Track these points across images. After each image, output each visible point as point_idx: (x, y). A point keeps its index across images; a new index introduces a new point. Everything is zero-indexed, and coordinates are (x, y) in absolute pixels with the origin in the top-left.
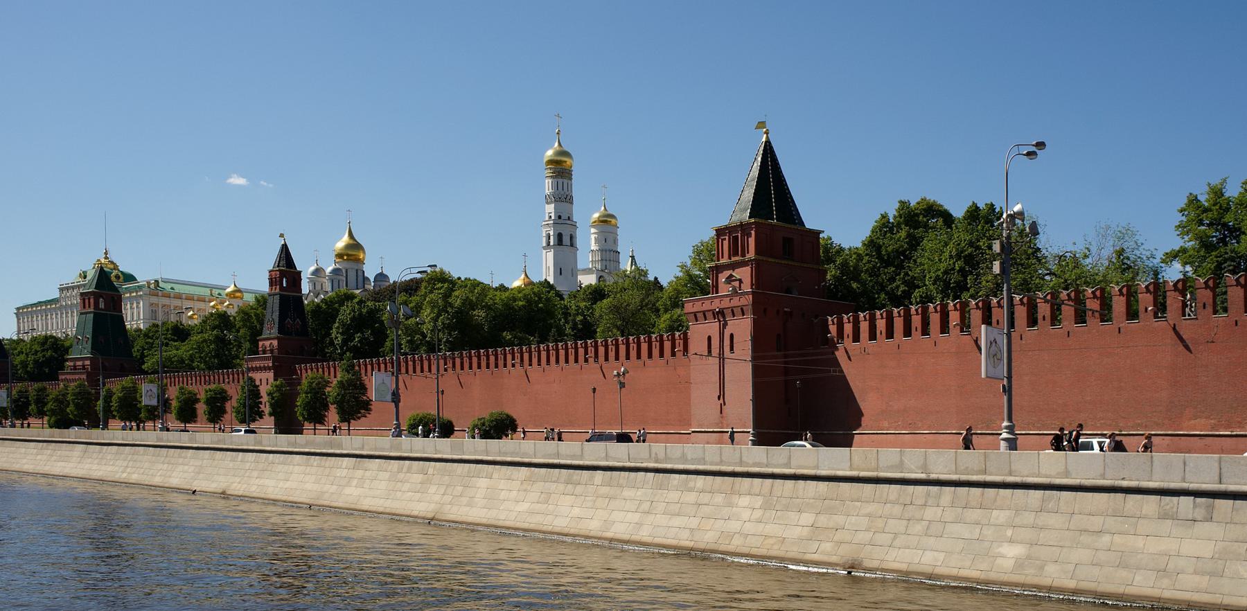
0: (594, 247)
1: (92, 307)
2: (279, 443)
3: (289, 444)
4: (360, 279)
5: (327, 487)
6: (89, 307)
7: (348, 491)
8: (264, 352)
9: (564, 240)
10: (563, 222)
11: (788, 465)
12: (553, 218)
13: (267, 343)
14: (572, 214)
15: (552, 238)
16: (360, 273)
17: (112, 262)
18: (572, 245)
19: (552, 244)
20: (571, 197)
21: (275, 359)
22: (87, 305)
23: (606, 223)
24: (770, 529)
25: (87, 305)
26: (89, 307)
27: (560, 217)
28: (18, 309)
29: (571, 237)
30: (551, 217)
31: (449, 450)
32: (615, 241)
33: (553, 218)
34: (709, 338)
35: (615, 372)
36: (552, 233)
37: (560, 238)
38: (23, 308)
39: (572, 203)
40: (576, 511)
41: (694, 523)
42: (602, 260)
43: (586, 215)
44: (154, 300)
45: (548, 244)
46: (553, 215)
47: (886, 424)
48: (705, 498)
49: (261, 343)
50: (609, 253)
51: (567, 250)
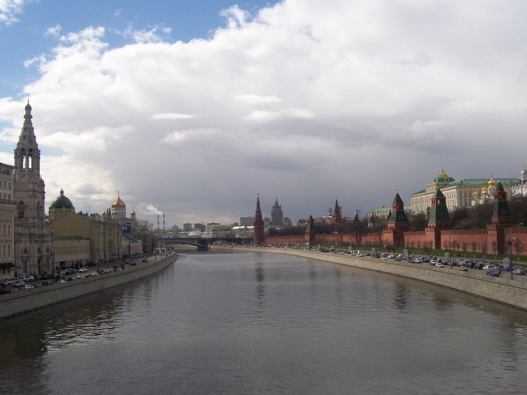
6: (435, 204)
7: (496, 294)
13: (494, 220)
21: (497, 226)
26: (435, 204)
44: (460, 189)
49: (492, 220)
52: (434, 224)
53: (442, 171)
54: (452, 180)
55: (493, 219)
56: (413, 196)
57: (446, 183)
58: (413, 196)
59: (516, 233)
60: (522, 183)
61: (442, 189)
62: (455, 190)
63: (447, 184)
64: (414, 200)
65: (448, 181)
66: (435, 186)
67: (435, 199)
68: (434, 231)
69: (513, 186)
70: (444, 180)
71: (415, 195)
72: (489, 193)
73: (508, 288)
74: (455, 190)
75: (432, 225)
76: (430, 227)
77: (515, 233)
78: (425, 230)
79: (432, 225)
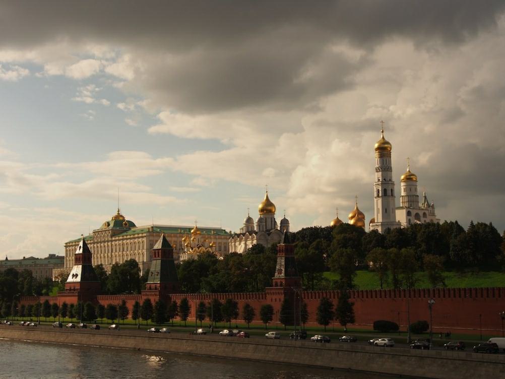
0: (403, 194)
1: (160, 257)
4: (273, 223)
6: (158, 256)
8: (276, 285)
9: (387, 191)
10: (387, 182)
12: (381, 180)
14: (391, 177)
15: (380, 192)
16: (273, 219)
17: (122, 216)
18: (392, 195)
19: (380, 195)
20: (391, 167)
22: (157, 256)
23: (410, 179)
25: (157, 256)
26: (158, 256)
27: (384, 180)
28: (66, 244)
29: (392, 190)
30: (379, 180)
32: (416, 190)
35: (500, 314)
36: (380, 189)
37: (385, 191)
38: (69, 243)
39: (392, 171)
42: (408, 201)
43: (398, 177)
45: (378, 196)
46: (380, 179)
49: (274, 281)
50: (412, 198)
51: (390, 198)
53: (118, 211)
54: (132, 225)
55: (274, 279)
59: (372, 297)
61: (119, 237)
64: (70, 250)
65: (127, 226)
66: (110, 231)
67: (160, 251)
74: (145, 239)
76: (150, 288)
77: (381, 297)
78: (142, 293)
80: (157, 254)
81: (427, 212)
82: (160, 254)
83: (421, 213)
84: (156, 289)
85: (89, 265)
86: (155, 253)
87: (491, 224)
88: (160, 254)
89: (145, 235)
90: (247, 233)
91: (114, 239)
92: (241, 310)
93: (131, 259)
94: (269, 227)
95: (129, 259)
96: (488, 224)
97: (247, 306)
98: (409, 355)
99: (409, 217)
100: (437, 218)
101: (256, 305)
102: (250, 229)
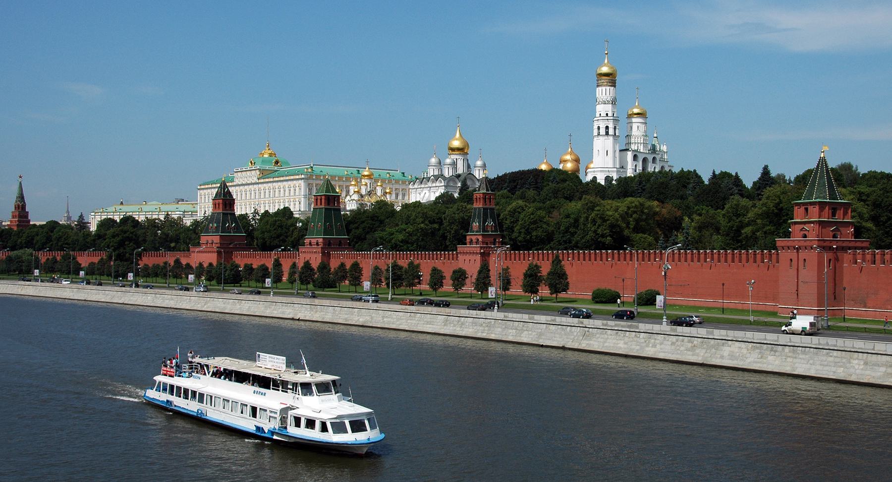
2: (590, 324)
3: (603, 325)
5: (633, 347)
6: (321, 204)
7: (647, 349)
8: (471, 242)
11: (874, 349)
24: (868, 372)
26: (321, 204)
27: (607, 114)
31: (705, 334)
33: (602, 115)
34: (791, 260)
37: (607, 128)
40: (777, 362)
41: (834, 369)
44: (310, 181)
47: (889, 307)
48: (838, 360)
49: (467, 237)
52: (321, 240)
56: (203, 187)
57: (276, 168)
58: (203, 187)
60: (432, 179)
62: (302, 182)
63: (277, 171)
67: (323, 197)
68: (320, 251)
69: (412, 183)
70: (272, 163)
71: (210, 186)
72: (363, 192)
73: (674, 339)
75: (314, 241)
76: (310, 244)
79: (314, 241)
80: (319, 201)
81: (658, 157)
82: (323, 200)
83: (650, 158)
84: (317, 244)
85: (230, 214)
86: (317, 200)
87: (737, 173)
88: (323, 200)
89: (303, 176)
90: (432, 177)
91: (262, 181)
92: (425, 273)
93: (285, 208)
94: (460, 171)
95: (282, 207)
96: (734, 174)
97: (435, 270)
98: (638, 331)
99: (635, 163)
100: (669, 164)
101: (446, 264)
102: (436, 173)
